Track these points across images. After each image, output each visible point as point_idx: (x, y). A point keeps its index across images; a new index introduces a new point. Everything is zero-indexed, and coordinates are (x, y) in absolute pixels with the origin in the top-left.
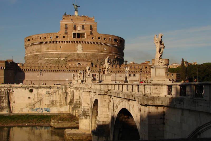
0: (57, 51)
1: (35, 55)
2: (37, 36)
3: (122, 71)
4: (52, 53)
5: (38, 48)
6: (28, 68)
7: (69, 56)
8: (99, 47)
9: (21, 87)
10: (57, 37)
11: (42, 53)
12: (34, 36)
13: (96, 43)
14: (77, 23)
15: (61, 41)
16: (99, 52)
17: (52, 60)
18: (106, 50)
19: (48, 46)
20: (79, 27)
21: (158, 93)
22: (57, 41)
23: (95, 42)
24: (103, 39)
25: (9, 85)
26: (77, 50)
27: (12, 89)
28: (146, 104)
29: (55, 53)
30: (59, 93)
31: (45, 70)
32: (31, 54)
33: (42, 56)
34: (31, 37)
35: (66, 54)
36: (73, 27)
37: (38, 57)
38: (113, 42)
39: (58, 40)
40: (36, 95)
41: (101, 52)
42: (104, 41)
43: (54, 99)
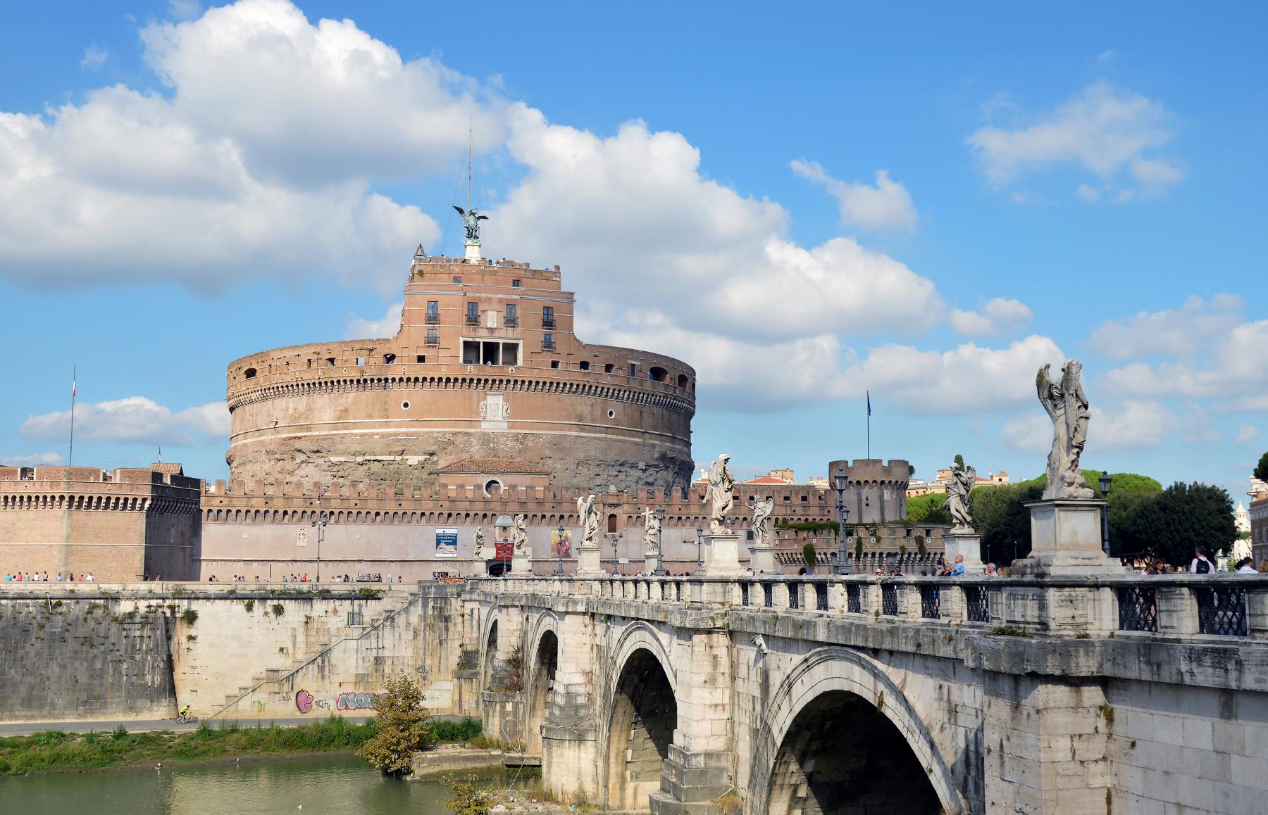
0: (387, 424)
4: (361, 435)
6: (254, 501)
7: (447, 444)
8: (582, 404)
9: (232, 592)
10: (390, 358)
11: (315, 433)
12: (276, 355)
14: (483, 295)
16: (582, 428)
17: (365, 467)
18: (617, 421)
20: (490, 313)
21: (1078, 620)
25: (171, 585)
27: (185, 602)
28: (1034, 669)
30: (408, 624)
32: (263, 438)
34: (261, 355)
37: (299, 451)
38: (648, 385)
39: (395, 370)
40: (301, 629)
42: (607, 380)
43: (386, 653)
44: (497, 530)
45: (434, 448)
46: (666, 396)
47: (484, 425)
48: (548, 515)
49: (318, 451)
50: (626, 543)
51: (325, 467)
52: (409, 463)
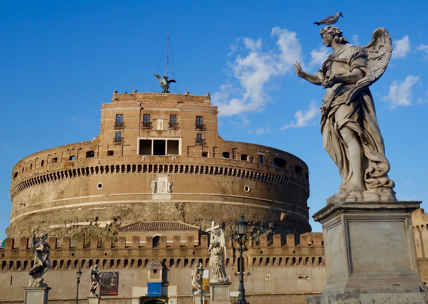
0: (87, 200)
1: (25, 218)
2: (33, 158)
3: (307, 258)
4: (71, 209)
5: (34, 195)
7: (125, 212)
13: (214, 169)
14: (154, 109)
15: (102, 167)
16: (225, 198)
19: (62, 185)
22: (87, 168)
23: (212, 168)
24: (238, 157)
29: (80, 207)
31: (22, 261)
33: (42, 220)
35: (116, 209)
36: (142, 121)
37: (32, 223)
38: (273, 171)
39: (94, 163)
41: (235, 199)
44: (149, 273)
46: (286, 178)
48: (190, 260)
49: (43, 222)
50: (253, 280)
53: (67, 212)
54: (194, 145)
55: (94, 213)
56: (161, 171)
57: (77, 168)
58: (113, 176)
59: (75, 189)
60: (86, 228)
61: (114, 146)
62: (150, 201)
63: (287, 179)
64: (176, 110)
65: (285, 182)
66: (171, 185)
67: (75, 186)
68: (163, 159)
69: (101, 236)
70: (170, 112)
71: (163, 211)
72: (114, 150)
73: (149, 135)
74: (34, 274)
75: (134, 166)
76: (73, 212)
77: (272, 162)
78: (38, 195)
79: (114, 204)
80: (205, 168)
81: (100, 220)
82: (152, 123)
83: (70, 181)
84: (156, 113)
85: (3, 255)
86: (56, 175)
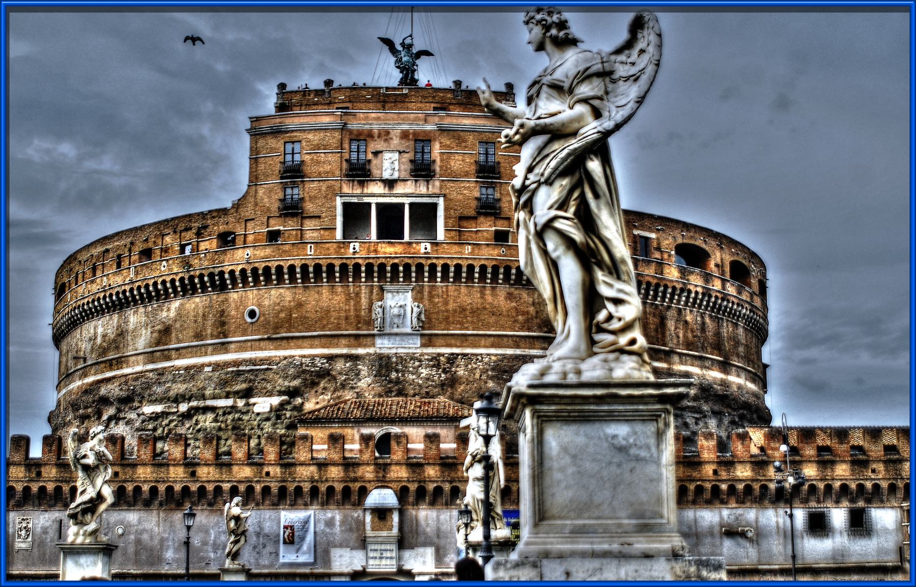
0: (224, 347)
4: (187, 368)
5: (104, 336)
7: (314, 377)
11: (126, 371)
19: (164, 314)
22: (222, 273)
26: (375, 332)
29: (209, 365)
33: (124, 394)
35: (291, 371)
37: (105, 401)
38: (672, 273)
44: (368, 518)
45: (296, 383)
46: (707, 293)
47: (379, 342)
51: (137, 424)
52: (257, 409)
53: (181, 375)
54: (472, 213)
55: (242, 378)
56: (394, 279)
57: (198, 273)
58: (282, 291)
59: (196, 321)
60: (224, 414)
61: (281, 220)
62: (371, 350)
63: (710, 296)
64: (429, 127)
65: (705, 303)
66: (420, 313)
67: (195, 316)
68: (398, 249)
69: (259, 433)
70: (415, 133)
71: (403, 375)
72: (281, 228)
73: (365, 191)
74: (80, 517)
75: (331, 267)
76: (192, 377)
77: (670, 256)
78: (112, 336)
79: (285, 358)
80: (502, 270)
81: (252, 396)
82: (369, 161)
83: (182, 305)
84: (379, 136)
85: (39, 474)
86: (151, 288)
